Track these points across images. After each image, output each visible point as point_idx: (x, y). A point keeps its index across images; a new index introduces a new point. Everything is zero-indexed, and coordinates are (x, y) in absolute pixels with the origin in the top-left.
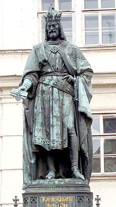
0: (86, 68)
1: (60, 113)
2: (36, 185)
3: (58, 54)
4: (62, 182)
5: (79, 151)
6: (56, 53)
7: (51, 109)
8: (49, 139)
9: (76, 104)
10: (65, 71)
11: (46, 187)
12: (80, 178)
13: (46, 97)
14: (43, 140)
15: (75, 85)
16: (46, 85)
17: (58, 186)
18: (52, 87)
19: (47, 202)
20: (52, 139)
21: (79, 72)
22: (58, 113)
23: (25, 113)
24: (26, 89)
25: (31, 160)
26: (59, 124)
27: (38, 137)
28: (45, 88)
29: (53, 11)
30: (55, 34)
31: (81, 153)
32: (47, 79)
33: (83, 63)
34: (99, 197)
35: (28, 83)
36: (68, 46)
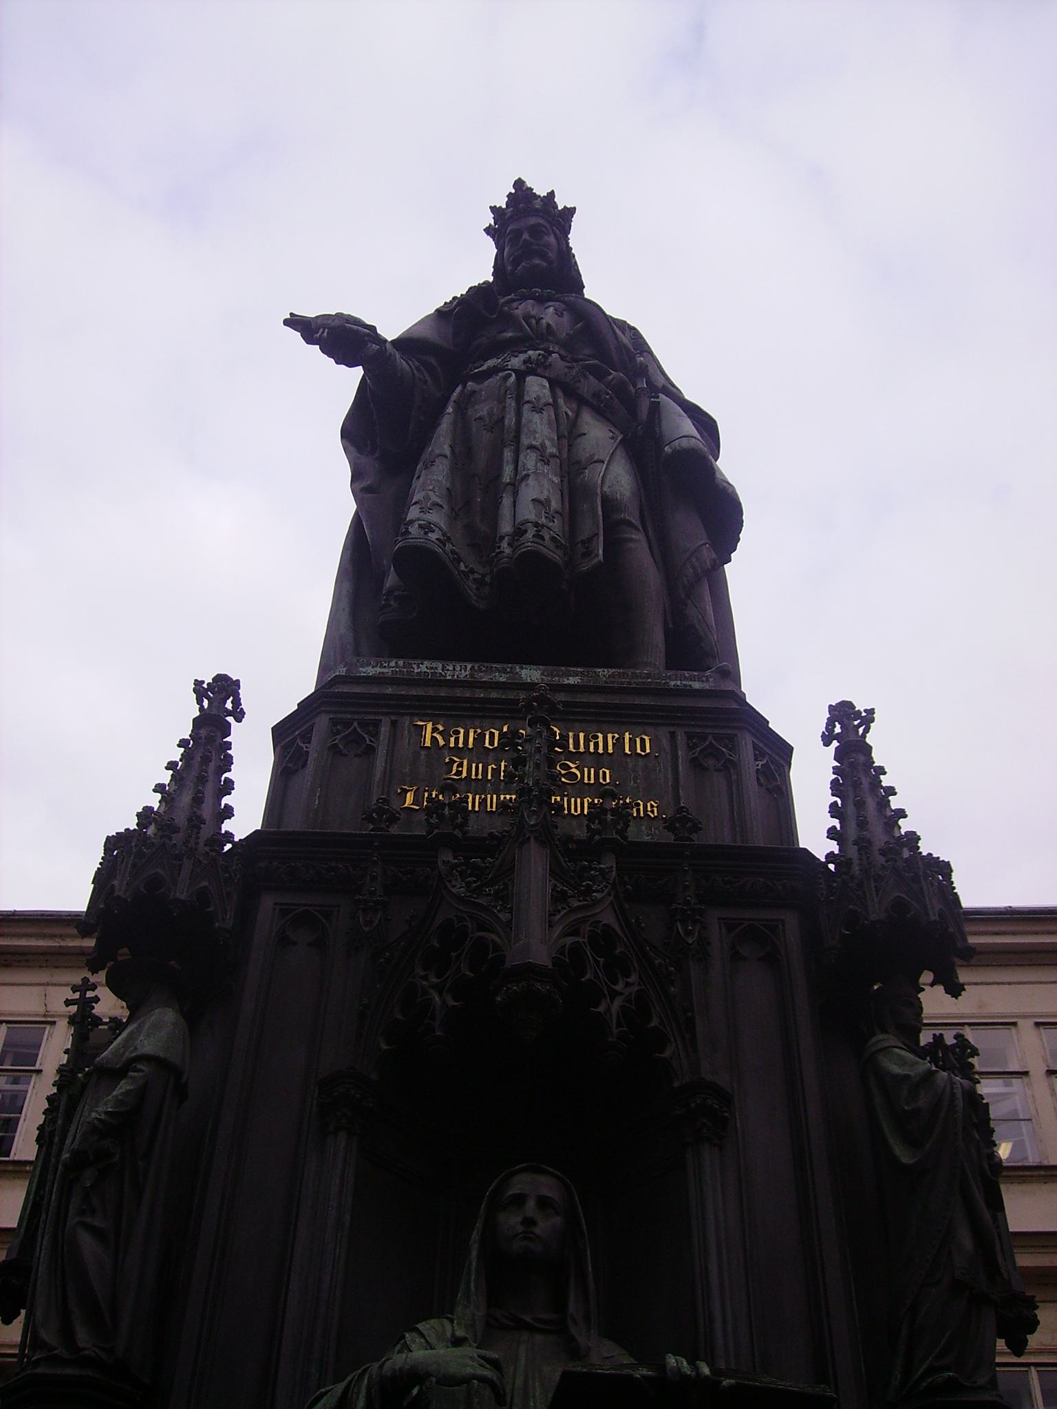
4: (568, 675)
5: (667, 632)
19: (457, 751)
26: (556, 480)
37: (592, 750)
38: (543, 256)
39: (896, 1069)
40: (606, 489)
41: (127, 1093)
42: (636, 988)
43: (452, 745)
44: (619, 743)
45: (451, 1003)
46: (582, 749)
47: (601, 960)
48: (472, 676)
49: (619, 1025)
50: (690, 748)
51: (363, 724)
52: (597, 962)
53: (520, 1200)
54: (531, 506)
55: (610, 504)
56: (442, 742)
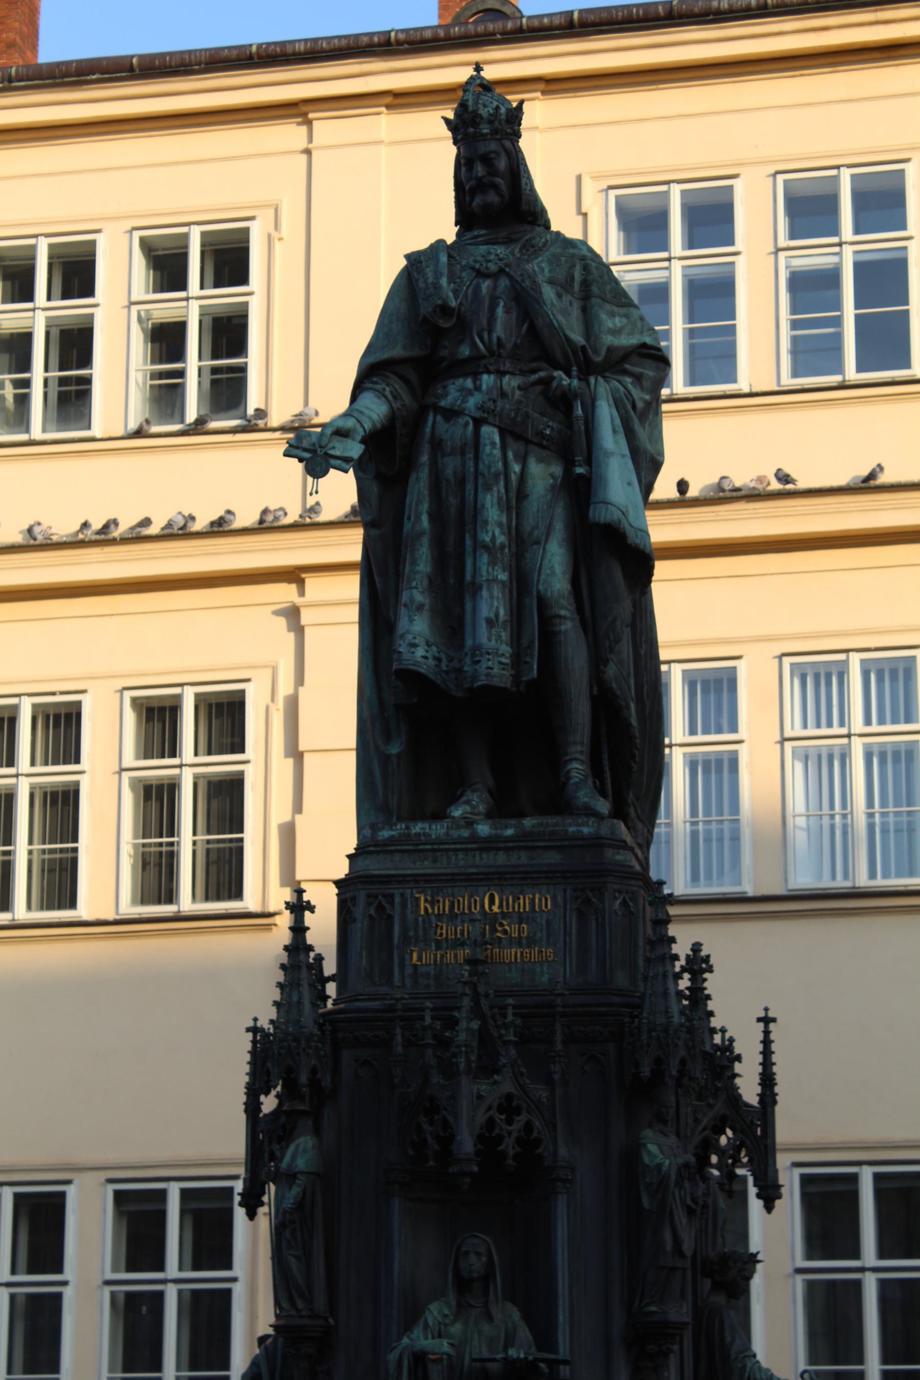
0: (634, 341)
2: (391, 841)
3: (504, 282)
4: (506, 827)
5: (592, 698)
8: (462, 646)
11: (437, 848)
13: (450, 465)
16: (451, 414)
17: (490, 845)
19: (439, 916)
20: (469, 642)
21: (598, 359)
24: (361, 433)
25: (388, 739)
26: (503, 576)
27: (409, 637)
29: (485, 98)
30: (493, 198)
31: (605, 704)
33: (618, 322)
37: (516, 910)
38: (495, 187)
39: (646, 1159)
40: (541, 587)
43: (436, 912)
44: (532, 901)
45: (437, 1147)
46: (511, 910)
47: (503, 1117)
48: (447, 834)
49: (514, 1148)
51: (384, 896)
52: (501, 1120)
54: (484, 625)
55: (543, 603)
56: (430, 911)
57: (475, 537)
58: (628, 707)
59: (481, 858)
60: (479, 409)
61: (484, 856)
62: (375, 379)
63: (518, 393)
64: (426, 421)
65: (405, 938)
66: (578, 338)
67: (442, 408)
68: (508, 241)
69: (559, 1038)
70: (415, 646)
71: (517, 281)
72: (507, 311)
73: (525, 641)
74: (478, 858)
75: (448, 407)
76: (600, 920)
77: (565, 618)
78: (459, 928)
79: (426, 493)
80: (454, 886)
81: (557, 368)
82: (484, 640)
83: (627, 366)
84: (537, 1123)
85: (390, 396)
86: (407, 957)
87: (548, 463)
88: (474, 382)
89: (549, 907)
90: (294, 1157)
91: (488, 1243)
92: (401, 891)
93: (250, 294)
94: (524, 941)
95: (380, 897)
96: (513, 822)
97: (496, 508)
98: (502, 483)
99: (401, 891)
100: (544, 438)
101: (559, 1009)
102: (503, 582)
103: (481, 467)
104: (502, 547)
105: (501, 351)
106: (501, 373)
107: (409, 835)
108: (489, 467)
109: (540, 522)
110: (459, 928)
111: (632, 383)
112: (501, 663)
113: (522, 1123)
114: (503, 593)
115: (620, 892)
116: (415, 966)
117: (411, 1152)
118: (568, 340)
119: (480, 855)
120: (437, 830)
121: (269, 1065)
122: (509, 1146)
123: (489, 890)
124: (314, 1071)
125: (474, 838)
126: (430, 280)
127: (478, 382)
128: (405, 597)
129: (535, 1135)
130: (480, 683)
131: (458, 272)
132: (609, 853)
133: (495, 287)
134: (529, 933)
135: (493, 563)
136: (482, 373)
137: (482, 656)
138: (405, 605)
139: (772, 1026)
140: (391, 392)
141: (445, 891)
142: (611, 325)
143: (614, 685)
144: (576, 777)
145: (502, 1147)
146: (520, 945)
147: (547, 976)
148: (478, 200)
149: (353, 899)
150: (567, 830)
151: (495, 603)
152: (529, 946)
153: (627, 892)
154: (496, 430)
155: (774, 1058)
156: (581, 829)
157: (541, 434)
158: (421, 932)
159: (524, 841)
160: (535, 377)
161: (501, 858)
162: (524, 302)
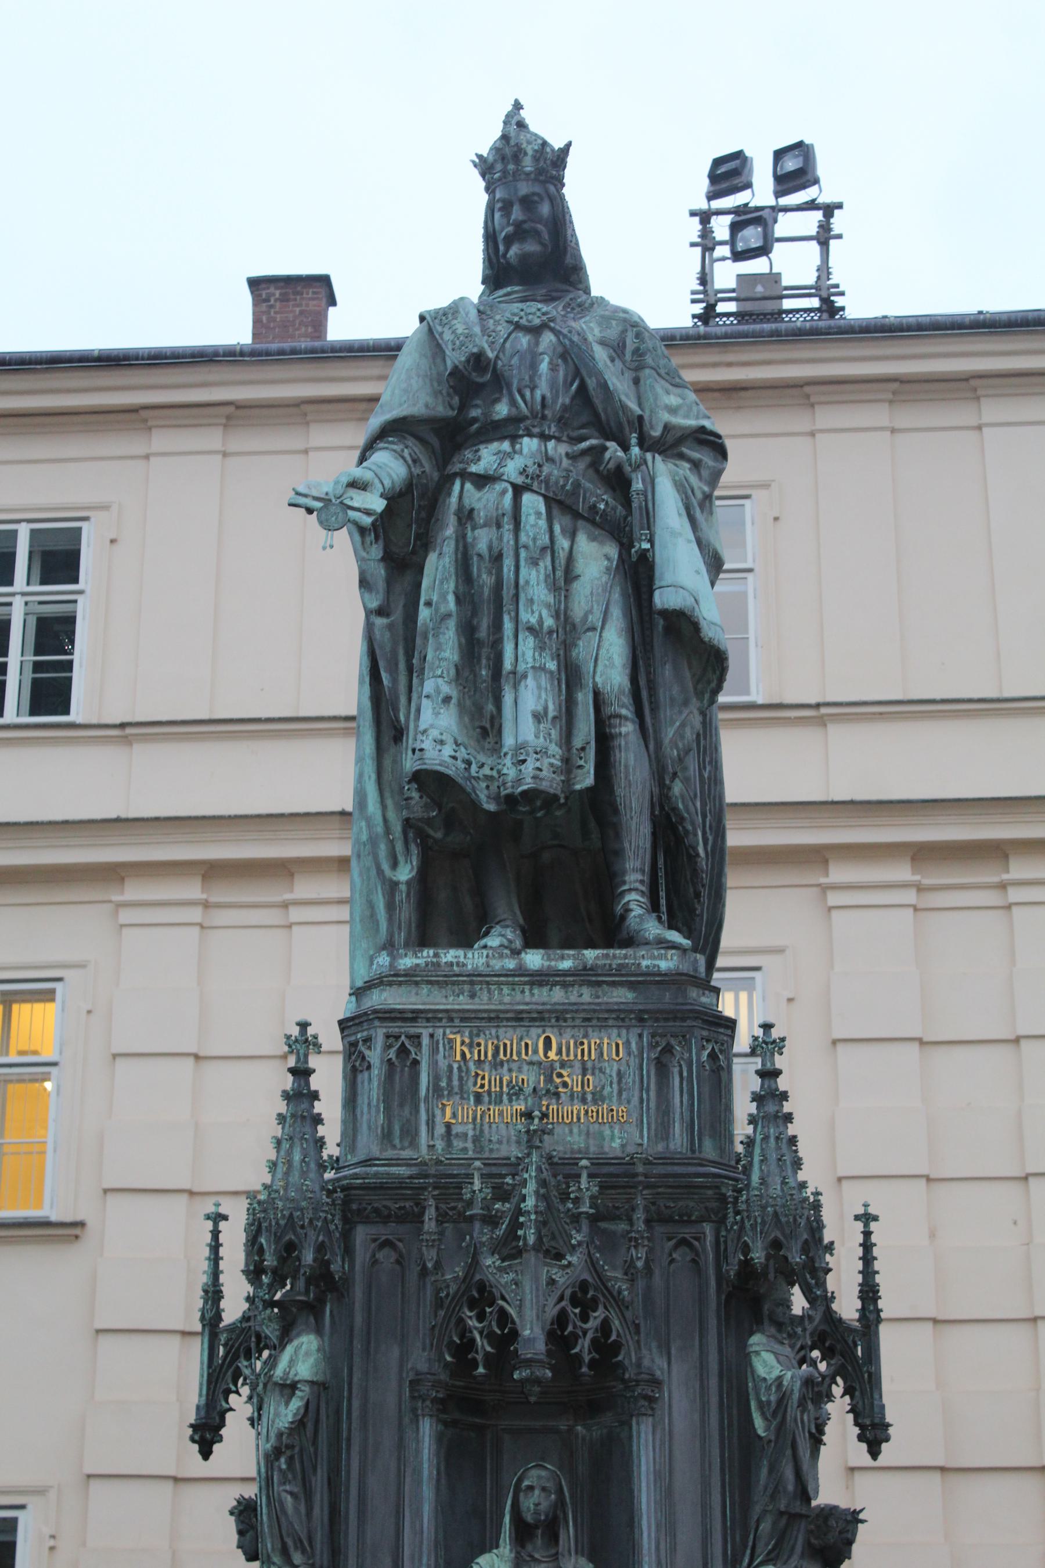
0: (692, 423)
1: (557, 616)
3: (548, 339)
4: (562, 958)
6: (535, 331)
7: (507, 593)
8: (496, 749)
9: (638, 574)
10: (585, 418)
11: (475, 979)
12: (664, 944)
13: (482, 540)
14: (462, 753)
15: (638, 485)
16: (483, 481)
17: (540, 978)
18: (518, 490)
20: (509, 741)
22: (545, 613)
23: (369, 627)
25: (395, 865)
26: (552, 666)
28: (473, 497)
30: (531, 247)
31: (668, 829)
32: (487, 457)
33: (673, 400)
34: (775, 1033)
35: (390, 466)
36: (599, 311)
39: (761, 1370)
40: (598, 679)
41: (298, 1409)
42: (603, 1316)
43: (476, 1058)
45: (489, 1349)
46: (572, 1057)
47: (577, 1311)
49: (590, 1352)
50: (652, 1046)
51: (409, 1037)
52: (575, 1314)
53: (531, 1488)
54: (530, 719)
56: (468, 1056)
57: (516, 620)
58: (696, 835)
59: (532, 995)
60: (521, 473)
61: (536, 991)
62: (391, 439)
63: (566, 462)
64: (449, 495)
65: (436, 1090)
66: (633, 405)
67: (471, 474)
68: (549, 299)
69: (640, 1215)
70: (442, 742)
71: (565, 336)
72: (553, 368)
73: (578, 742)
74: (527, 993)
75: (482, 472)
76: (685, 1074)
77: (626, 718)
78: (506, 1079)
79: (452, 570)
80: (498, 1026)
81: (608, 439)
82: (531, 738)
83: (685, 450)
84: (617, 1322)
85: (408, 459)
86: (438, 1112)
87: (602, 543)
88: (513, 446)
89: (621, 1055)
90: (292, 1362)
91: (558, 1476)
92: (431, 1030)
93: (81, 592)
94: (589, 1097)
95: (403, 1038)
96: (571, 952)
97: (543, 585)
98: (549, 558)
99: (431, 1030)
100: (597, 513)
101: (641, 1178)
102: (551, 672)
103: (523, 538)
104: (550, 632)
105: (546, 412)
106: (544, 437)
107: (438, 964)
108: (535, 539)
109: (595, 607)
110: (506, 1079)
111: (690, 469)
112: (552, 765)
113: (598, 1321)
114: (552, 684)
115: (708, 1041)
116: (448, 1126)
117: (448, 1358)
118: (624, 407)
119: (531, 990)
120: (474, 959)
121: (263, 1241)
122: (583, 1347)
123: (544, 1032)
124: (320, 1248)
125: (521, 971)
126: (459, 331)
127: (518, 447)
128: (429, 686)
129: (613, 1337)
130: (525, 787)
131: (492, 327)
132: (693, 993)
133: (537, 344)
134: (595, 1087)
135: (541, 648)
136: (522, 436)
137: (528, 755)
138: (427, 697)
139: (873, 1226)
140: (410, 454)
141: (487, 1032)
142: (667, 402)
143: (681, 806)
144: (637, 911)
145: (576, 1350)
146: (584, 1101)
147: (618, 1141)
148: (514, 250)
149: (367, 1040)
150: (639, 964)
151: (543, 696)
152: (595, 1102)
153: (716, 1043)
154: (541, 499)
155: (877, 1265)
156: (656, 962)
157: (593, 508)
158: (456, 1083)
159: (585, 976)
160: (585, 445)
161: (558, 995)
162: (572, 358)
